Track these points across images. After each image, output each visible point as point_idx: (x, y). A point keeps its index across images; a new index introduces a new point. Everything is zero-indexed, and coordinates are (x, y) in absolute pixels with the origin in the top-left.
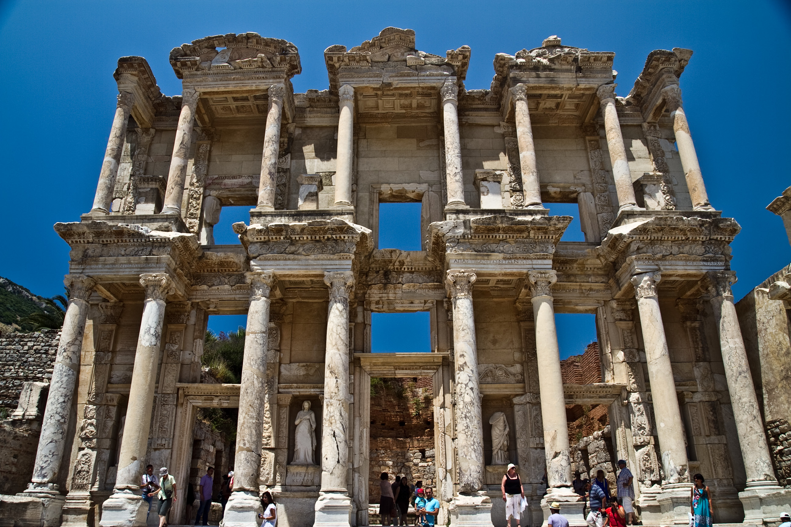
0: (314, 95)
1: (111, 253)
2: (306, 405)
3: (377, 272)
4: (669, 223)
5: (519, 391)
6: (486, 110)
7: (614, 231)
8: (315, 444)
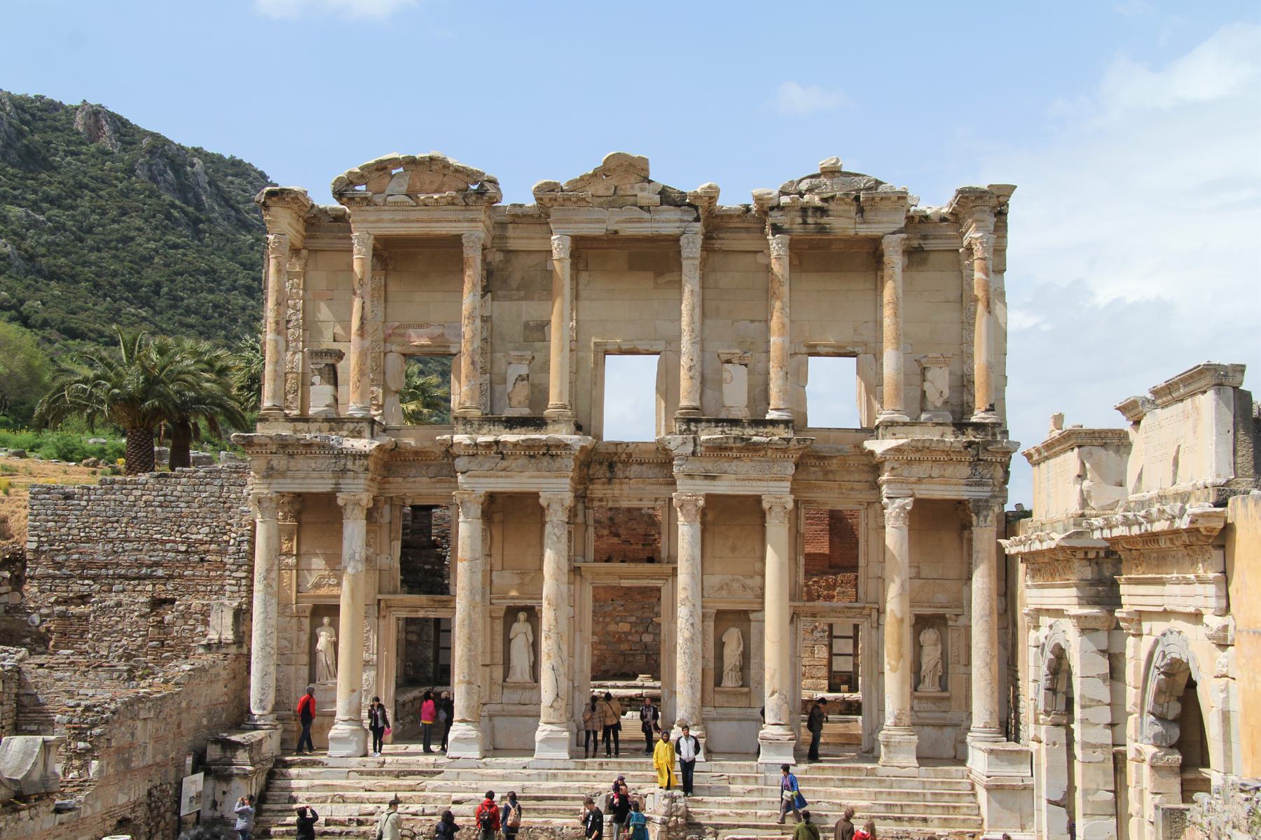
0: (519, 211)
1: (299, 466)
2: (522, 616)
3: (601, 464)
4: (927, 444)
5: (756, 607)
6: (747, 230)
7: (869, 445)
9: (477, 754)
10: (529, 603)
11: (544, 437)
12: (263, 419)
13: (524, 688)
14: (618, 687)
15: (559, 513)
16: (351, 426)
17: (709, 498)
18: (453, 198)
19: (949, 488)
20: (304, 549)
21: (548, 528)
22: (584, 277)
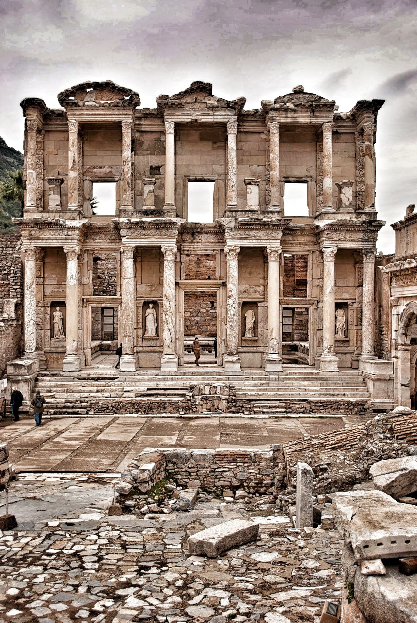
1: (45, 234)
2: (151, 305)
3: (188, 233)
7: (317, 223)
8: (156, 325)
9: (134, 370)
10: (154, 299)
11: (163, 219)
12: (27, 212)
13: (153, 339)
14: (187, 341)
15: (171, 256)
16: (69, 214)
17: (242, 248)
18: (118, 103)
19: (353, 243)
20: (46, 275)
21: (166, 263)
22: (179, 143)
